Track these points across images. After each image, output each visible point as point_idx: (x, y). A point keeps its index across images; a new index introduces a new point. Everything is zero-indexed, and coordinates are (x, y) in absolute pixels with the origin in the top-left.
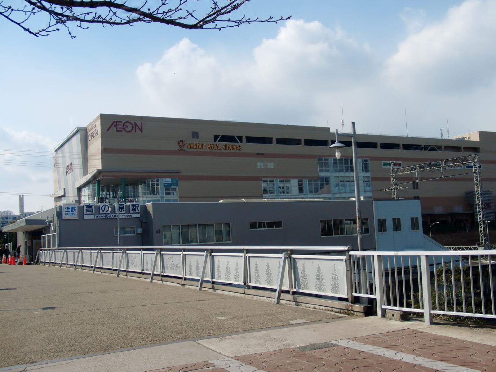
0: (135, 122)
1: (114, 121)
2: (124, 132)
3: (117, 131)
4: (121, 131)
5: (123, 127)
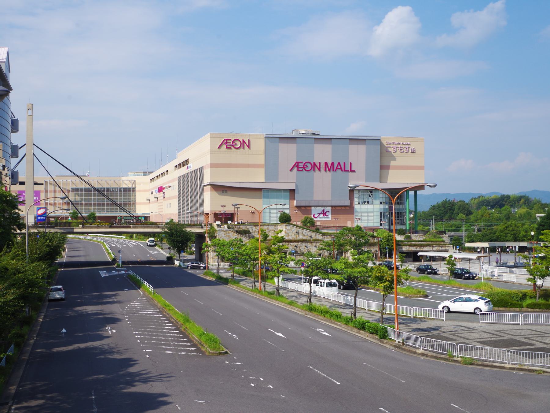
0: (243, 140)
1: (225, 139)
2: (232, 147)
3: (227, 148)
4: (230, 148)
5: (232, 144)
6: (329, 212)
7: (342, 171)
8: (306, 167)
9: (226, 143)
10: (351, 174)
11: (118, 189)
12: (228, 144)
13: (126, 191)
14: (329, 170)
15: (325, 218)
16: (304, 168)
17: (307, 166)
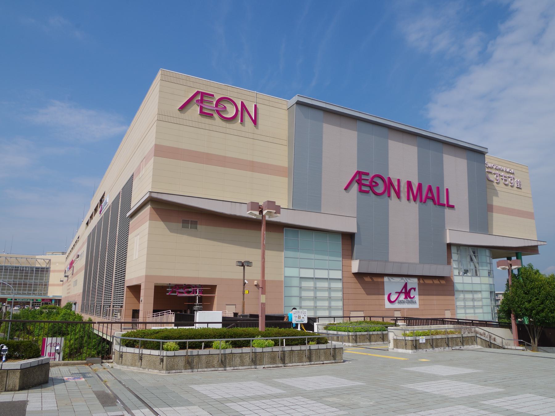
0: (242, 104)
1: (198, 93)
2: (216, 115)
4: (210, 116)
6: (415, 289)
7: (435, 204)
8: (375, 186)
9: (202, 101)
10: (447, 211)
11: (29, 268)
12: (205, 105)
13: (38, 271)
14: (415, 200)
15: (409, 302)
16: (371, 187)
17: (377, 184)
